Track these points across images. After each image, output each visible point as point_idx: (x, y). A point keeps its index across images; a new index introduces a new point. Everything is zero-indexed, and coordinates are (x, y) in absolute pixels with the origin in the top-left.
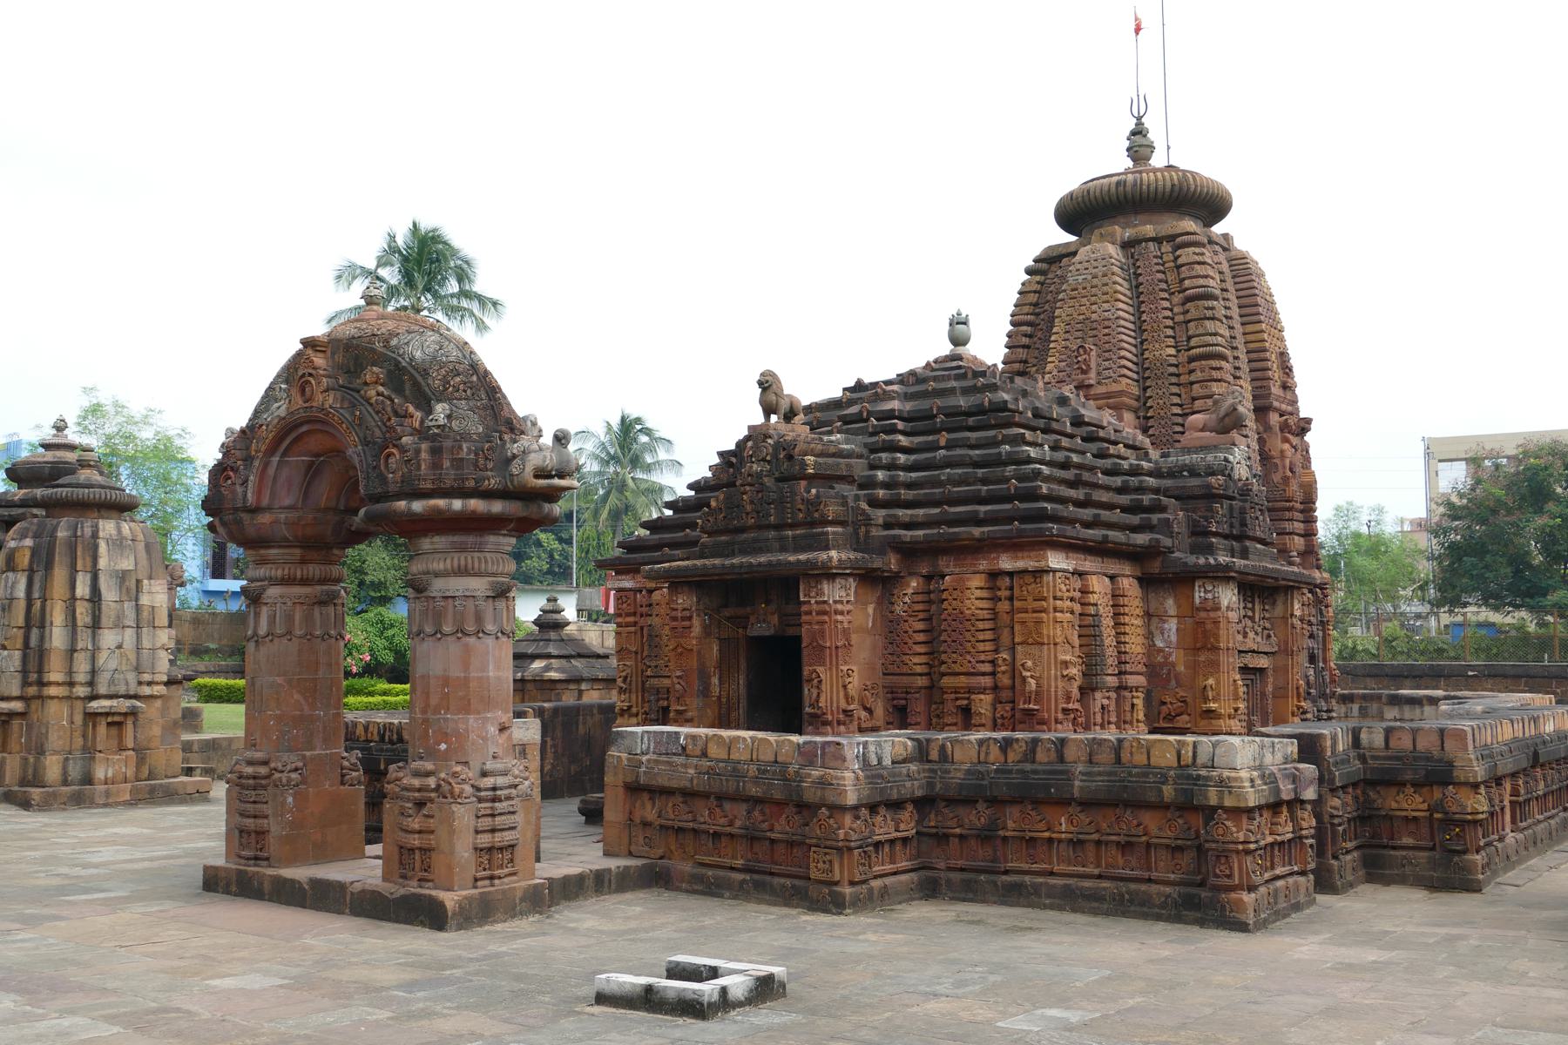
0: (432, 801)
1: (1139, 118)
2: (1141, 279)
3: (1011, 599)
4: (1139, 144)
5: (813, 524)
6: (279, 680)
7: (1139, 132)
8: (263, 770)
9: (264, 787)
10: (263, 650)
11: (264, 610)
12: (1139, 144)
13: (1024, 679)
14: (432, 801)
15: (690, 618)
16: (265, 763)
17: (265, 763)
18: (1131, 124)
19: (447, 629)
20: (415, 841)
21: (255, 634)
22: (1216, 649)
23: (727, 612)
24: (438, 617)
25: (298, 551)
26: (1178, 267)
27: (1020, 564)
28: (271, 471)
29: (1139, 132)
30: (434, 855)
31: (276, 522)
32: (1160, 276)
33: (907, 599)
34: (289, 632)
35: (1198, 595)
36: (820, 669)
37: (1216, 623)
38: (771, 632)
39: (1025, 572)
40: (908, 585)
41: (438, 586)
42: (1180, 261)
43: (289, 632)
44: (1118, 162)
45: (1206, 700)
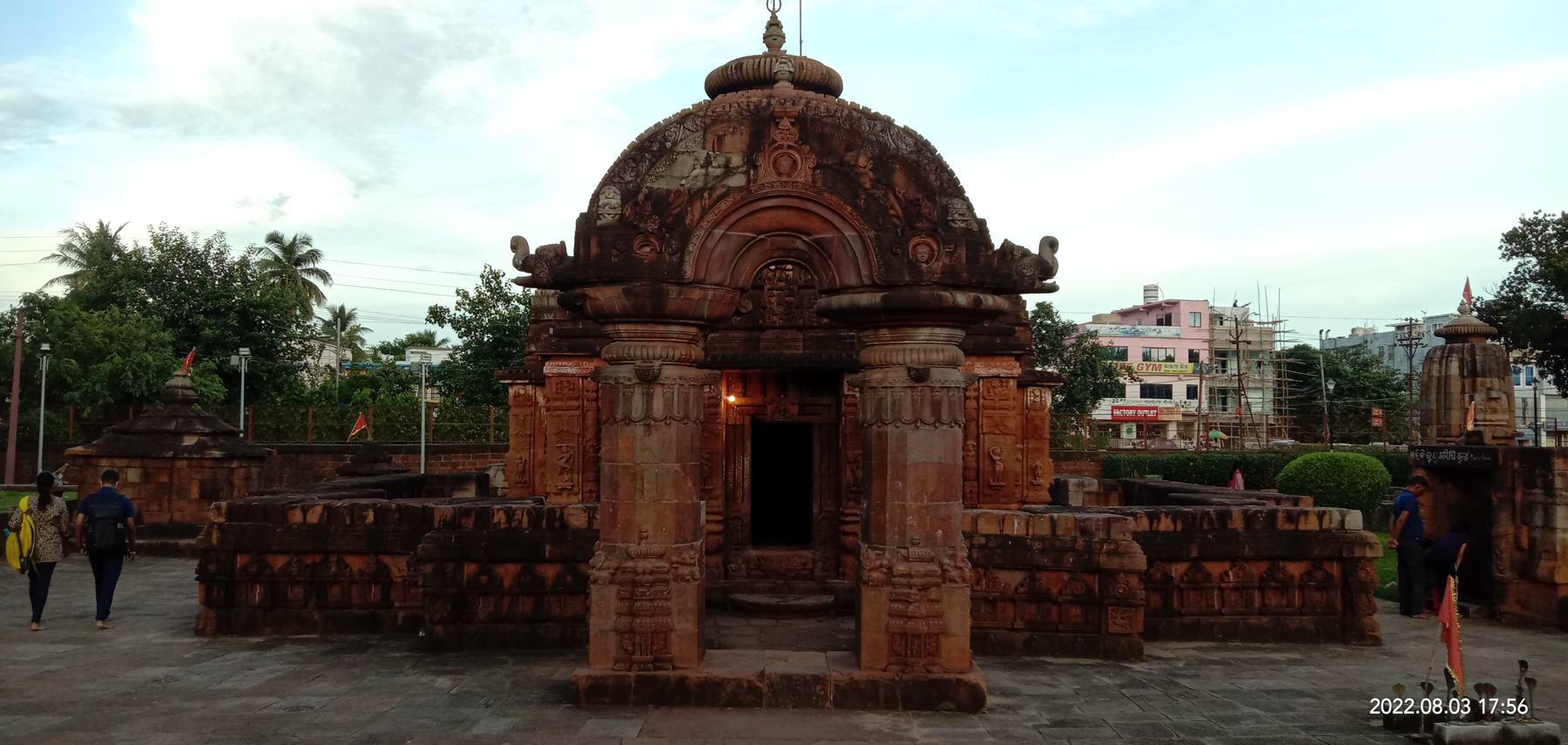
0: (938, 585)
1: (773, 13)
3: (977, 399)
4: (774, 33)
6: (677, 467)
7: (774, 26)
9: (666, 582)
10: (655, 436)
12: (774, 33)
13: (994, 461)
14: (938, 585)
16: (660, 557)
17: (660, 557)
18: (767, 17)
19: (945, 417)
20: (922, 627)
21: (648, 414)
22: (1041, 438)
24: (936, 407)
25: (694, 330)
27: (994, 371)
28: (710, 244)
29: (774, 26)
30: (943, 640)
31: (705, 298)
34: (686, 416)
35: (1030, 398)
37: (1042, 420)
39: (997, 377)
41: (937, 374)
43: (686, 416)
44: (761, 49)
45: (1035, 476)
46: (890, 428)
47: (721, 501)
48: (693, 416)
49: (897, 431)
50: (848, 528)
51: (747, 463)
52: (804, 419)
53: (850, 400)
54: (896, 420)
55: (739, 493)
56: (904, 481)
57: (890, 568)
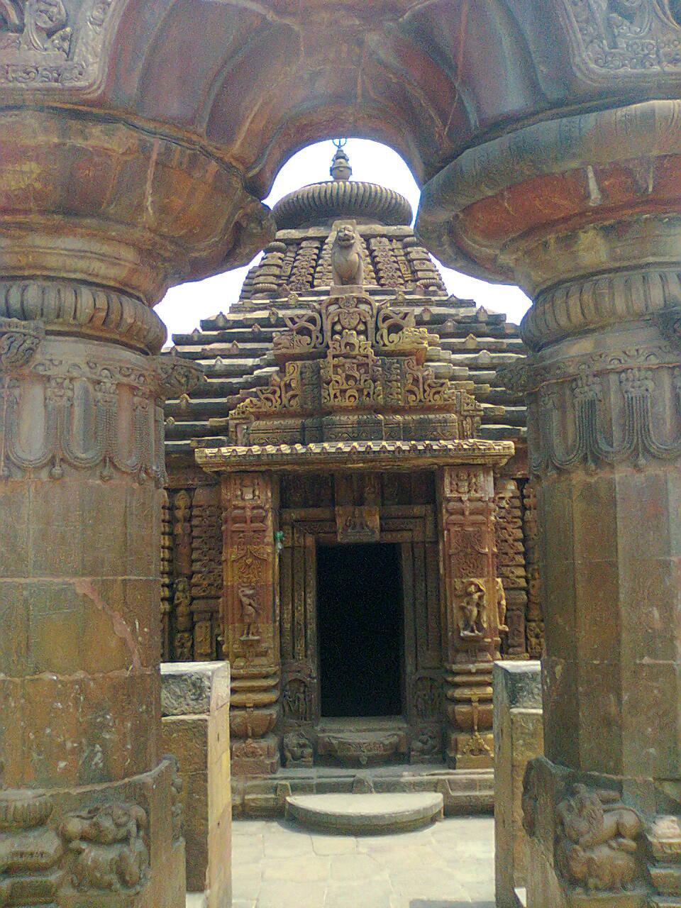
2: (380, 266)
5: (430, 409)
6: (82, 585)
8: (46, 844)
11: (35, 395)
15: (263, 520)
16: (36, 821)
17: (36, 821)
23: (294, 514)
25: (129, 254)
26: (410, 261)
32: (396, 265)
33: (504, 504)
34: (108, 460)
36: (480, 581)
38: (377, 537)
40: (504, 488)
42: (413, 256)
43: (108, 460)
46: (621, 474)
47: (274, 655)
48: (129, 462)
49: (639, 478)
50: (458, 693)
51: (311, 601)
52: (389, 538)
53: (452, 505)
54: (639, 449)
55: (300, 647)
56: (667, 608)
57: (640, 837)
